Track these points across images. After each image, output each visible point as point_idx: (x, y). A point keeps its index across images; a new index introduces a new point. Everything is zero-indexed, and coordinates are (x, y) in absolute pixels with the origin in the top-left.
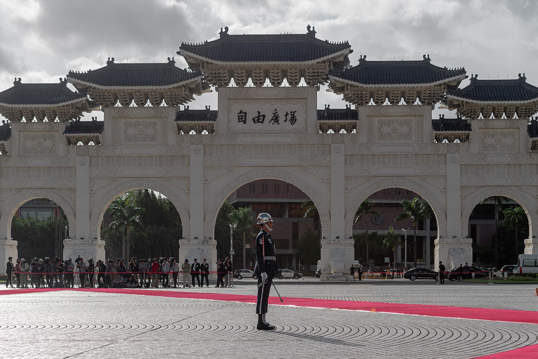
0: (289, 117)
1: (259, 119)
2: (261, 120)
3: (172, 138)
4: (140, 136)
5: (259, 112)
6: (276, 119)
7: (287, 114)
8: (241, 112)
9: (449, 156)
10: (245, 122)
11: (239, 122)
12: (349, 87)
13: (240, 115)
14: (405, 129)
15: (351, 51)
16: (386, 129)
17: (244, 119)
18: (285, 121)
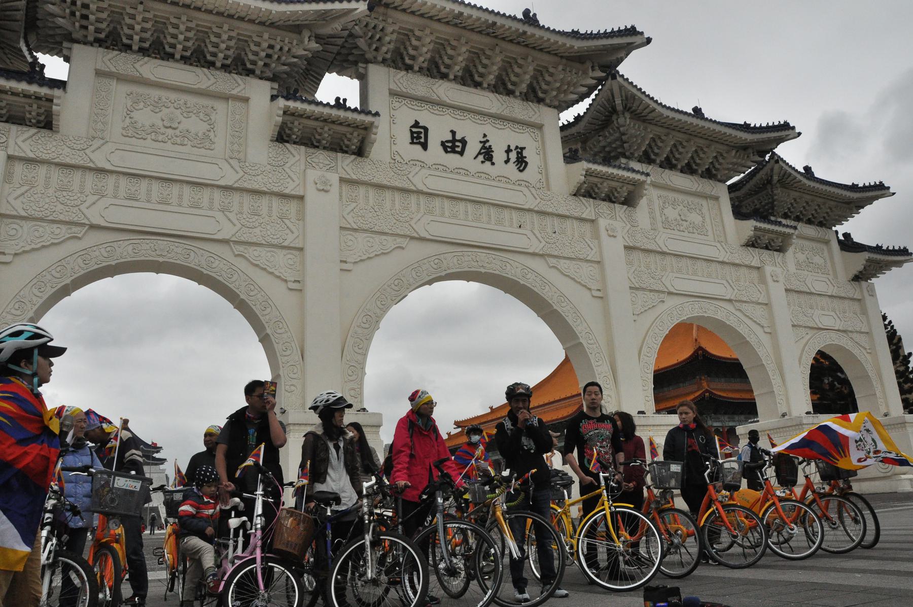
0: (513, 156)
1: (454, 146)
2: (457, 149)
3: (260, 149)
4: (170, 131)
5: (453, 133)
6: (487, 154)
7: (508, 151)
8: (416, 124)
9: (768, 269)
10: (425, 146)
11: (412, 143)
12: (627, 115)
13: (414, 130)
14: (695, 218)
15: (649, 40)
16: (671, 213)
17: (422, 140)
18: (507, 162)
